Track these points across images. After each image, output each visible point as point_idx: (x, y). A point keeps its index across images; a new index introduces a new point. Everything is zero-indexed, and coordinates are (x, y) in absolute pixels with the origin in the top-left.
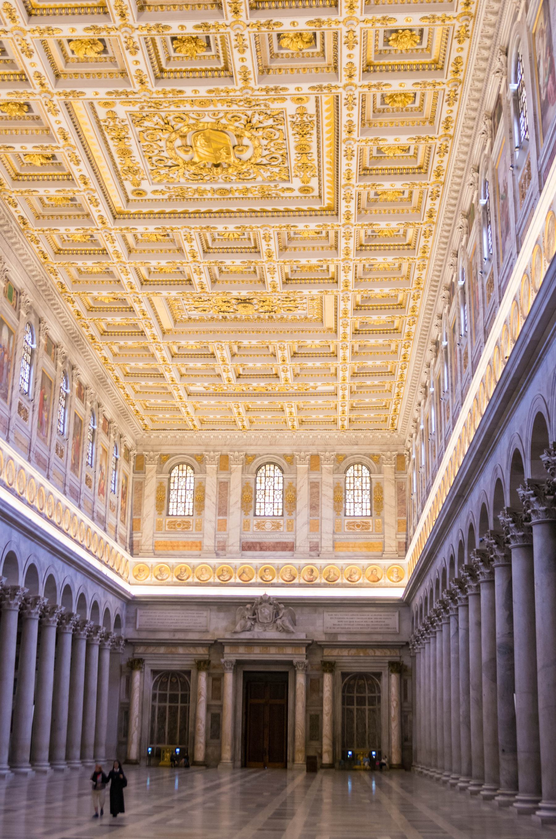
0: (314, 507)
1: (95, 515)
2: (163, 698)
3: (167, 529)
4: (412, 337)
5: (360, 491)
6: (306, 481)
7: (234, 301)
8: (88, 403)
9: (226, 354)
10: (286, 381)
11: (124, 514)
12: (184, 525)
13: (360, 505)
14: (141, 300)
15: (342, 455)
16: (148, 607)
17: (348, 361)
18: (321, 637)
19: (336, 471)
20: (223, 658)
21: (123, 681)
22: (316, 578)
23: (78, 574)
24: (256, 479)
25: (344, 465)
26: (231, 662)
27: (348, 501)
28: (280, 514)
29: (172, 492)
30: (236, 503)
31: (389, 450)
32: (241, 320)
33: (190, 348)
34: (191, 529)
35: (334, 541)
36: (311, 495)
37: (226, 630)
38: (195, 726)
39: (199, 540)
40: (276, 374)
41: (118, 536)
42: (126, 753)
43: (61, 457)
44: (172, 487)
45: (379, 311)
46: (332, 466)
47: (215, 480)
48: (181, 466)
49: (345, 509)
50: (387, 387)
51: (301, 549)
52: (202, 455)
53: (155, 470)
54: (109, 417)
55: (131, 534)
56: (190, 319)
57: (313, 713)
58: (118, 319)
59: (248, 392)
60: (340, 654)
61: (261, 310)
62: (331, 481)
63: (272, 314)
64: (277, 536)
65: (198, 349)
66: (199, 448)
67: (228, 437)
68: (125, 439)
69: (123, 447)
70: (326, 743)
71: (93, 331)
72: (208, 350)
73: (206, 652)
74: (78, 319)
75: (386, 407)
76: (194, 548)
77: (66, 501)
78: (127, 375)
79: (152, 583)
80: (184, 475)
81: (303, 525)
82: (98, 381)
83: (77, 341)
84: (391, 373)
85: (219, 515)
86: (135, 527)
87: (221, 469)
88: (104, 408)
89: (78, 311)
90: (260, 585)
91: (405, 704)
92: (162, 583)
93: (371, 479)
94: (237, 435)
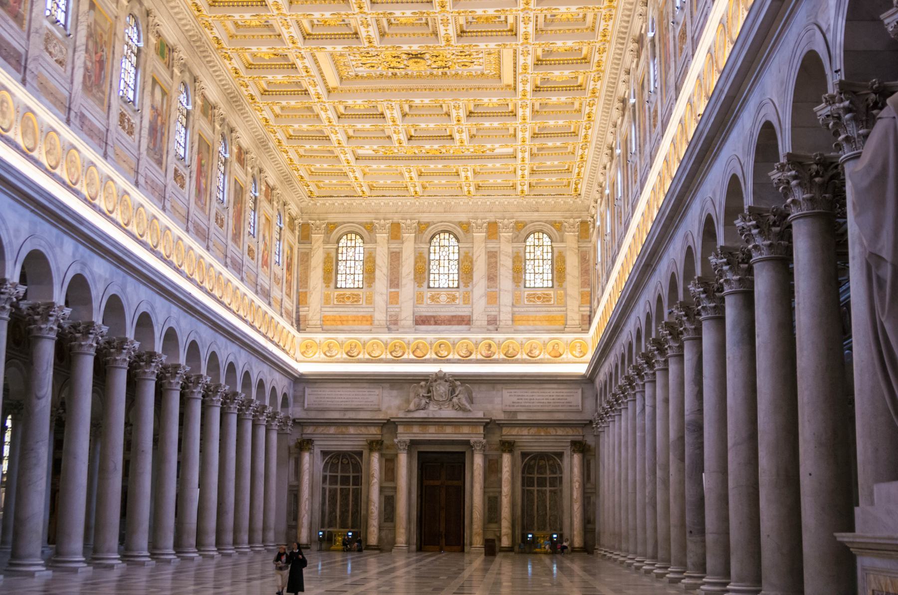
0: (492, 278)
1: (259, 288)
2: (333, 480)
3: (335, 303)
4: (597, 94)
5: (541, 261)
6: (484, 250)
7: (404, 56)
8: (249, 169)
9: (397, 114)
10: (462, 142)
11: (290, 287)
12: (353, 298)
13: (541, 276)
14: (304, 56)
15: (521, 222)
16: (317, 385)
17: (528, 121)
18: (499, 416)
19: (515, 239)
20: (397, 438)
21: (292, 462)
22: (494, 353)
23: (242, 351)
24: (429, 249)
25: (523, 233)
26: (405, 442)
27: (527, 271)
28: (456, 285)
29: (340, 263)
30: (408, 275)
31: (571, 217)
32: (412, 77)
33: (357, 107)
34: (361, 303)
35: (513, 314)
36: (489, 265)
37: (399, 408)
38: (367, 510)
39: (370, 314)
40: (451, 136)
41: (283, 311)
42: (296, 537)
43: (221, 226)
44: (340, 258)
45: (561, 66)
46: (511, 234)
47: (386, 251)
48: (349, 236)
49: (525, 280)
50: (570, 149)
52: (372, 223)
53: (322, 240)
54: (271, 183)
55: (298, 308)
56: (357, 76)
57: (491, 494)
58: (279, 77)
59: (420, 154)
60: (520, 433)
61: (434, 66)
62: (510, 250)
63: (446, 70)
64: (453, 309)
65: (366, 109)
66: (368, 215)
67: (400, 204)
68: (290, 207)
69: (287, 215)
70: (505, 525)
71: (253, 90)
72: (378, 111)
73: (379, 432)
74: (236, 78)
75: (569, 171)
76: (365, 322)
77: (227, 274)
78: (290, 138)
79: (320, 360)
80: (353, 244)
81: (480, 298)
82: (260, 145)
83: (236, 101)
84: (575, 134)
85: (391, 287)
86: (301, 300)
87: (392, 238)
88: (266, 174)
89: (236, 69)
90: (435, 361)
91: (589, 486)
92: (331, 360)
93: (552, 248)
94: (409, 201)
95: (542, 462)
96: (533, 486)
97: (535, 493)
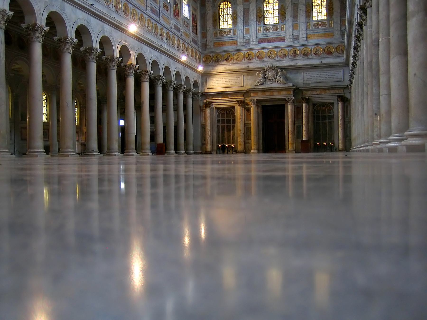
2: (223, 121)
23: (162, 55)
34: (231, 35)
37: (251, 85)
51: (289, 40)
95: (324, 108)
96: (320, 120)
97: (321, 123)
